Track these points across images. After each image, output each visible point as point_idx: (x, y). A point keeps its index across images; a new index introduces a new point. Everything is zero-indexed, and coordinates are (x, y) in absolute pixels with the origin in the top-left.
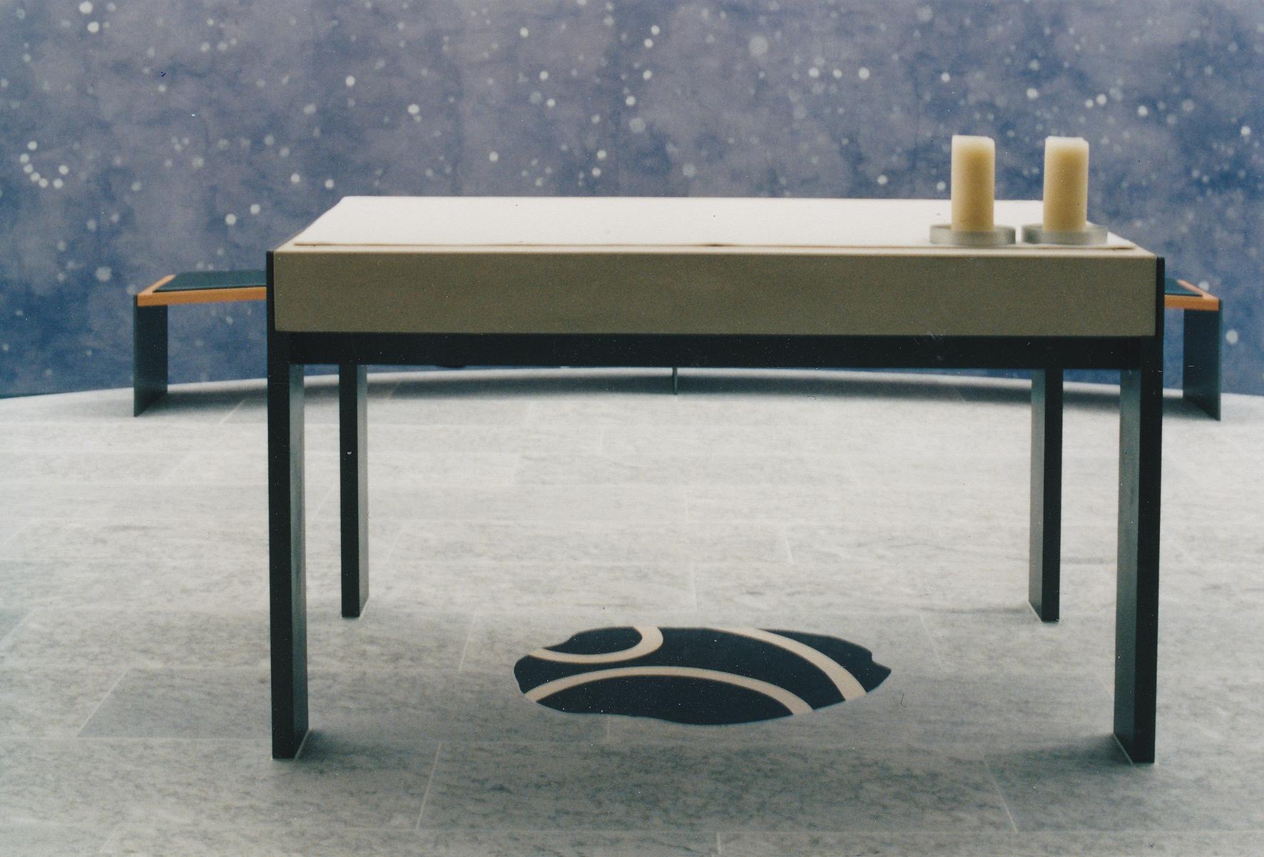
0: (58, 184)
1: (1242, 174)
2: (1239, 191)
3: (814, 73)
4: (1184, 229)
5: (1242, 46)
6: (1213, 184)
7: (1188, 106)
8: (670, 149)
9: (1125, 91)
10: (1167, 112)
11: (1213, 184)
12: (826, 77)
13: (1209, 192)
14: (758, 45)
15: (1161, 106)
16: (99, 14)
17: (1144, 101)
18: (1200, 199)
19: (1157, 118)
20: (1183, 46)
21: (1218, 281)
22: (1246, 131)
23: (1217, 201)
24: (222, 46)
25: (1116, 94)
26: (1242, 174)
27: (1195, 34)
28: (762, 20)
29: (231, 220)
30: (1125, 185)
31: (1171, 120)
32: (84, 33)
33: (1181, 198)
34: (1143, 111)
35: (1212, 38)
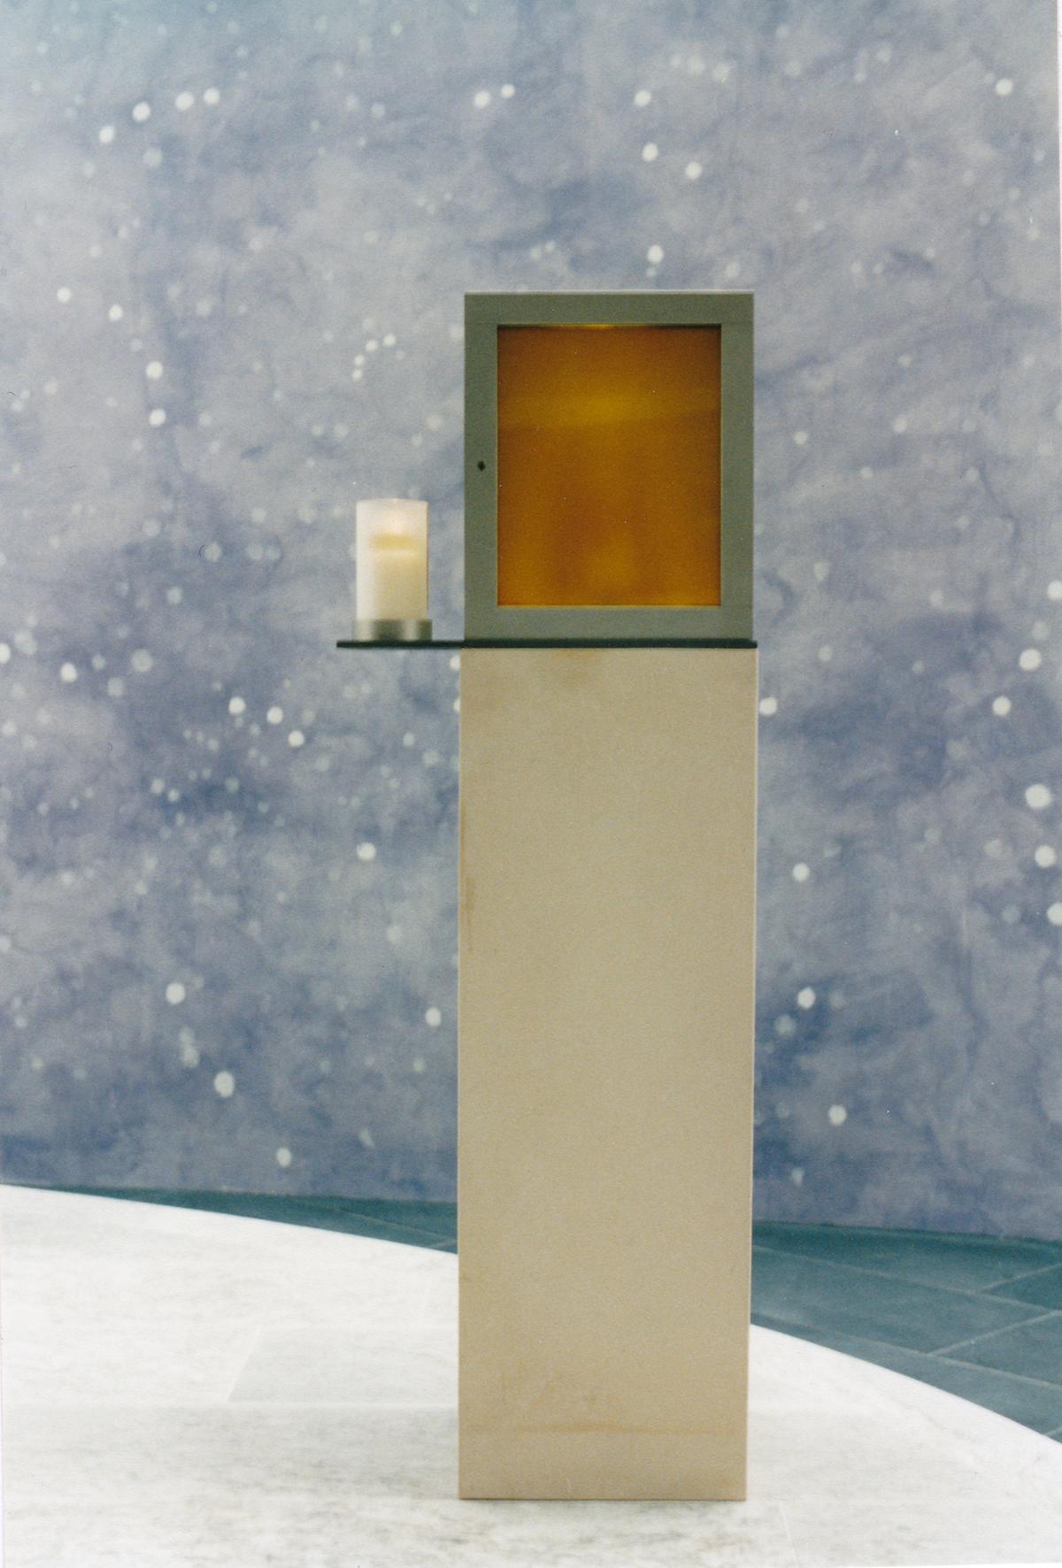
1: (233, 785)
2: (229, 816)
4: (141, 888)
5: (229, 549)
6: (185, 804)
7: (142, 662)
9: (40, 635)
10: (106, 675)
11: (185, 804)
13: (180, 819)
15: (99, 662)
17: (68, 655)
18: (166, 833)
19: (92, 686)
20: (132, 551)
21: (199, 982)
22: (237, 706)
23: (193, 837)
25: (26, 642)
26: (233, 785)
27: (152, 529)
30: (43, 808)
31: (115, 688)
33: (133, 831)
34: (69, 672)
35: (179, 534)
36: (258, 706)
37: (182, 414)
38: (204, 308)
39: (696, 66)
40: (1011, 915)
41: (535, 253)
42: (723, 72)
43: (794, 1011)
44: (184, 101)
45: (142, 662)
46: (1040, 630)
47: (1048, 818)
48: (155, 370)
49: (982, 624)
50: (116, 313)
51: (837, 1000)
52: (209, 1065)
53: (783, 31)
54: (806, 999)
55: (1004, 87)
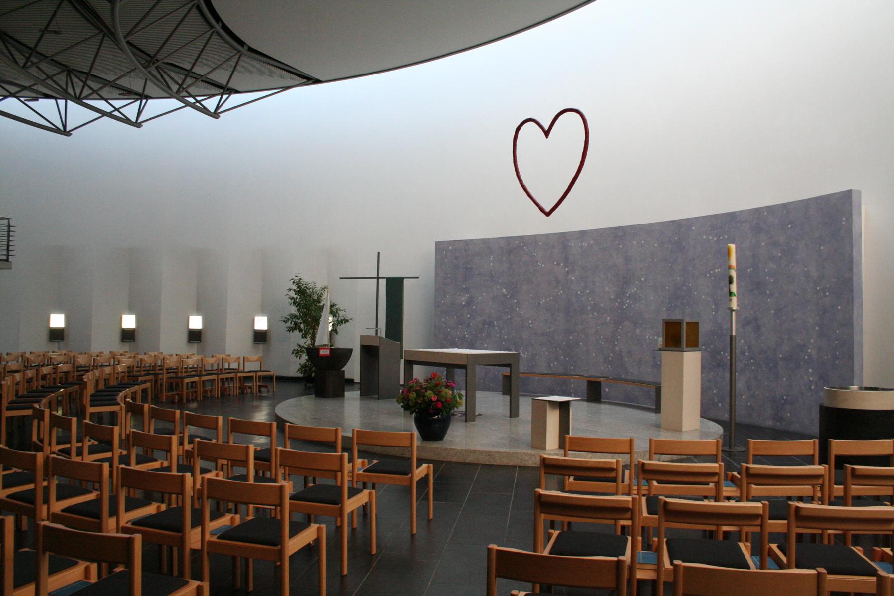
0: (526, 356)
1: (722, 364)
3: (647, 337)
7: (712, 346)
8: (623, 354)
12: (649, 338)
13: (716, 368)
14: (638, 331)
15: (707, 346)
16: (532, 323)
22: (722, 353)
24: (551, 330)
26: (722, 364)
27: (713, 328)
28: (638, 325)
29: (552, 365)
31: (709, 349)
32: (530, 327)
36: (724, 353)
37: (716, 313)
38: (719, 298)
39: (772, 266)
40: (807, 387)
41: (755, 292)
42: (775, 267)
43: (783, 399)
44: (716, 270)
45: (712, 346)
46: (810, 347)
47: (812, 373)
48: (713, 307)
49: (804, 345)
50: (709, 299)
51: (788, 398)
52: (719, 402)
53: (781, 261)
54: (785, 398)
55: (806, 269)
